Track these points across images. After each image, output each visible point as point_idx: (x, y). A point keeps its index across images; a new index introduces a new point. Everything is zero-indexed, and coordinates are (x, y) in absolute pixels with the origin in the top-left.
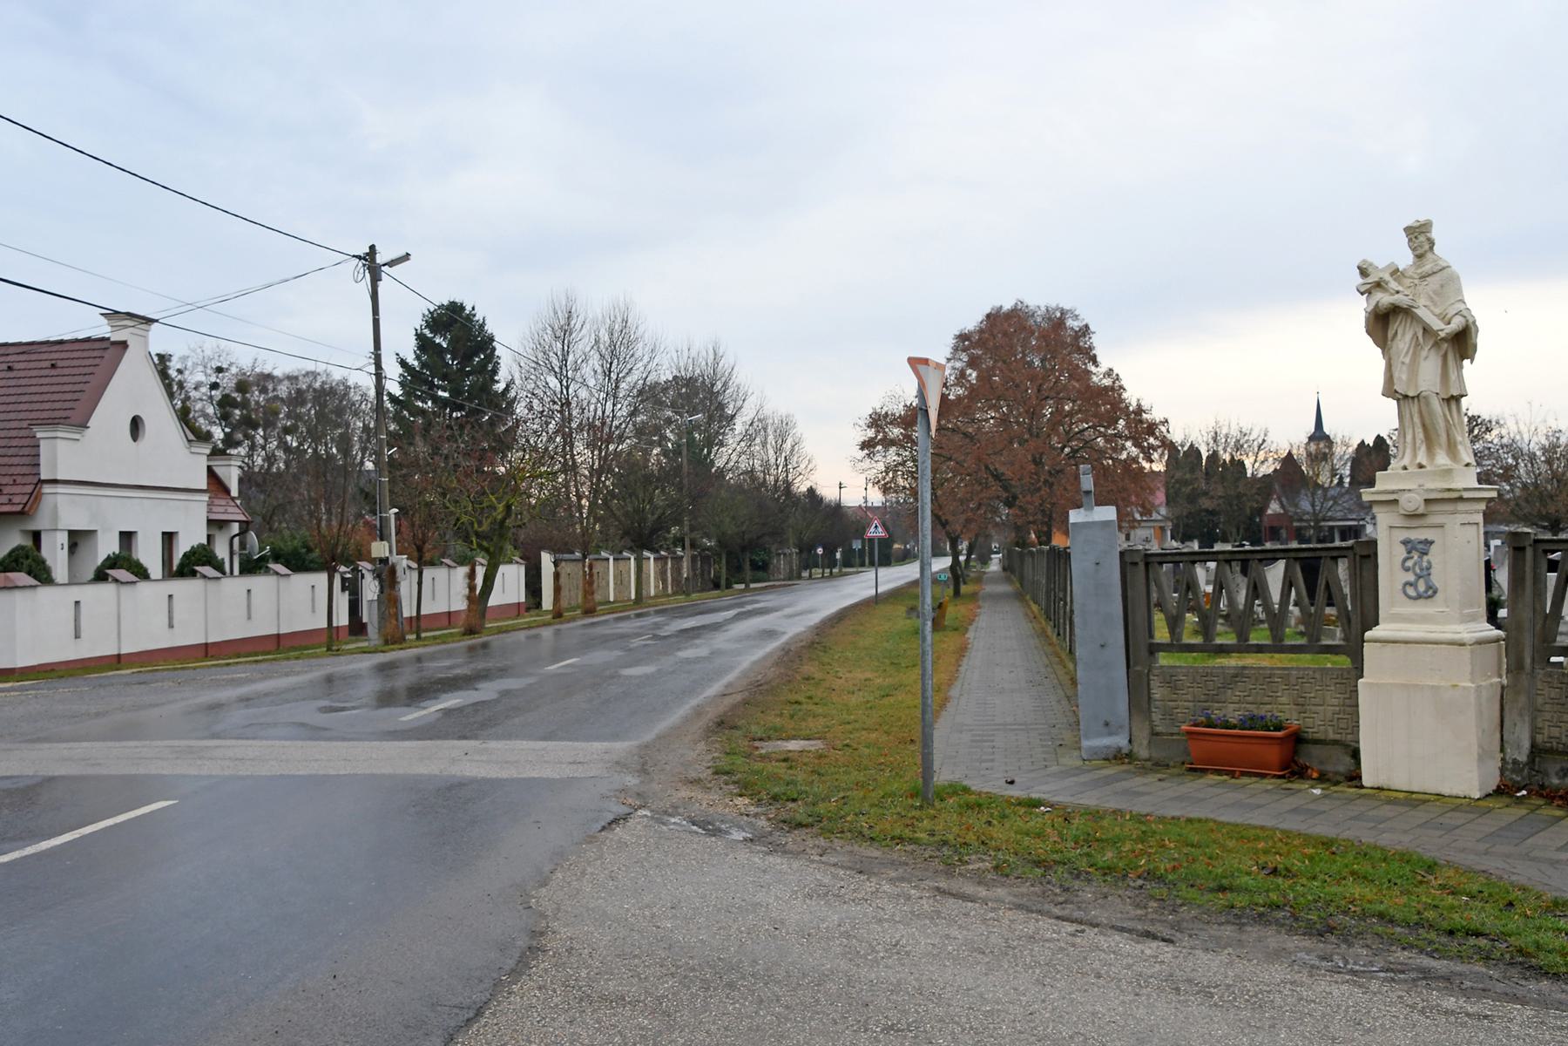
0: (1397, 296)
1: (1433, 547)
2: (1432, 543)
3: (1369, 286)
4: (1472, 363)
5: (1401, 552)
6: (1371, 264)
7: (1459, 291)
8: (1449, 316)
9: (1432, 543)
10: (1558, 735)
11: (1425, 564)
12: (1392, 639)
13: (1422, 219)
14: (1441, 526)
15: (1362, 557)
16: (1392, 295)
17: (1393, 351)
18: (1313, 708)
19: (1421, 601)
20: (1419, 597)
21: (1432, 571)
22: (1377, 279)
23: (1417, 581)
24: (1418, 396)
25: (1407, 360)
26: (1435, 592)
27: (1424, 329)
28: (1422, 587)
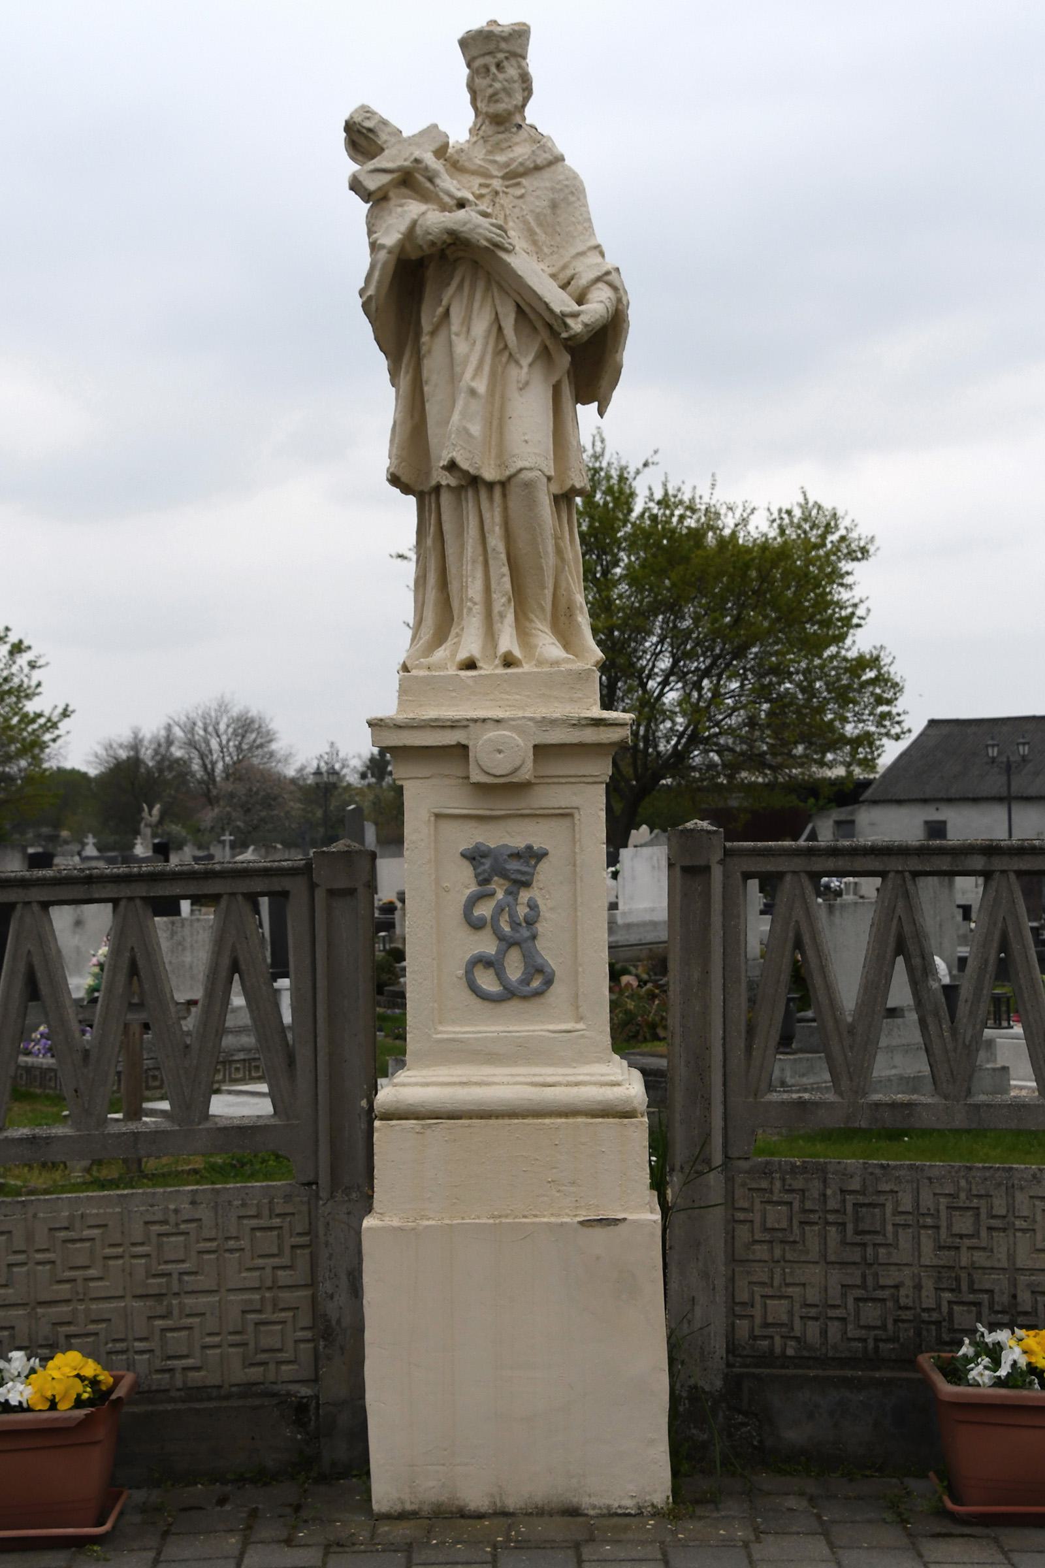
0: (461, 214)
1: (543, 866)
2: (540, 856)
3: (385, 178)
4: (601, 412)
5: (463, 879)
6: (385, 123)
7: (589, 228)
8: (584, 280)
9: (540, 856)
10: (784, 1318)
11: (522, 911)
12: (449, 1107)
13: (507, 19)
14: (566, 815)
15: (332, 893)
16: (444, 208)
17: (433, 366)
18: (189, 1301)
19: (513, 1006)
20: (509, 994)
21: (540, 927)
22: (400, 163)
23: (502, 953)
24: (504, 484)
25: (481, 387)
26: (549, 982)
27: (519, 308)
28: (514, 970)
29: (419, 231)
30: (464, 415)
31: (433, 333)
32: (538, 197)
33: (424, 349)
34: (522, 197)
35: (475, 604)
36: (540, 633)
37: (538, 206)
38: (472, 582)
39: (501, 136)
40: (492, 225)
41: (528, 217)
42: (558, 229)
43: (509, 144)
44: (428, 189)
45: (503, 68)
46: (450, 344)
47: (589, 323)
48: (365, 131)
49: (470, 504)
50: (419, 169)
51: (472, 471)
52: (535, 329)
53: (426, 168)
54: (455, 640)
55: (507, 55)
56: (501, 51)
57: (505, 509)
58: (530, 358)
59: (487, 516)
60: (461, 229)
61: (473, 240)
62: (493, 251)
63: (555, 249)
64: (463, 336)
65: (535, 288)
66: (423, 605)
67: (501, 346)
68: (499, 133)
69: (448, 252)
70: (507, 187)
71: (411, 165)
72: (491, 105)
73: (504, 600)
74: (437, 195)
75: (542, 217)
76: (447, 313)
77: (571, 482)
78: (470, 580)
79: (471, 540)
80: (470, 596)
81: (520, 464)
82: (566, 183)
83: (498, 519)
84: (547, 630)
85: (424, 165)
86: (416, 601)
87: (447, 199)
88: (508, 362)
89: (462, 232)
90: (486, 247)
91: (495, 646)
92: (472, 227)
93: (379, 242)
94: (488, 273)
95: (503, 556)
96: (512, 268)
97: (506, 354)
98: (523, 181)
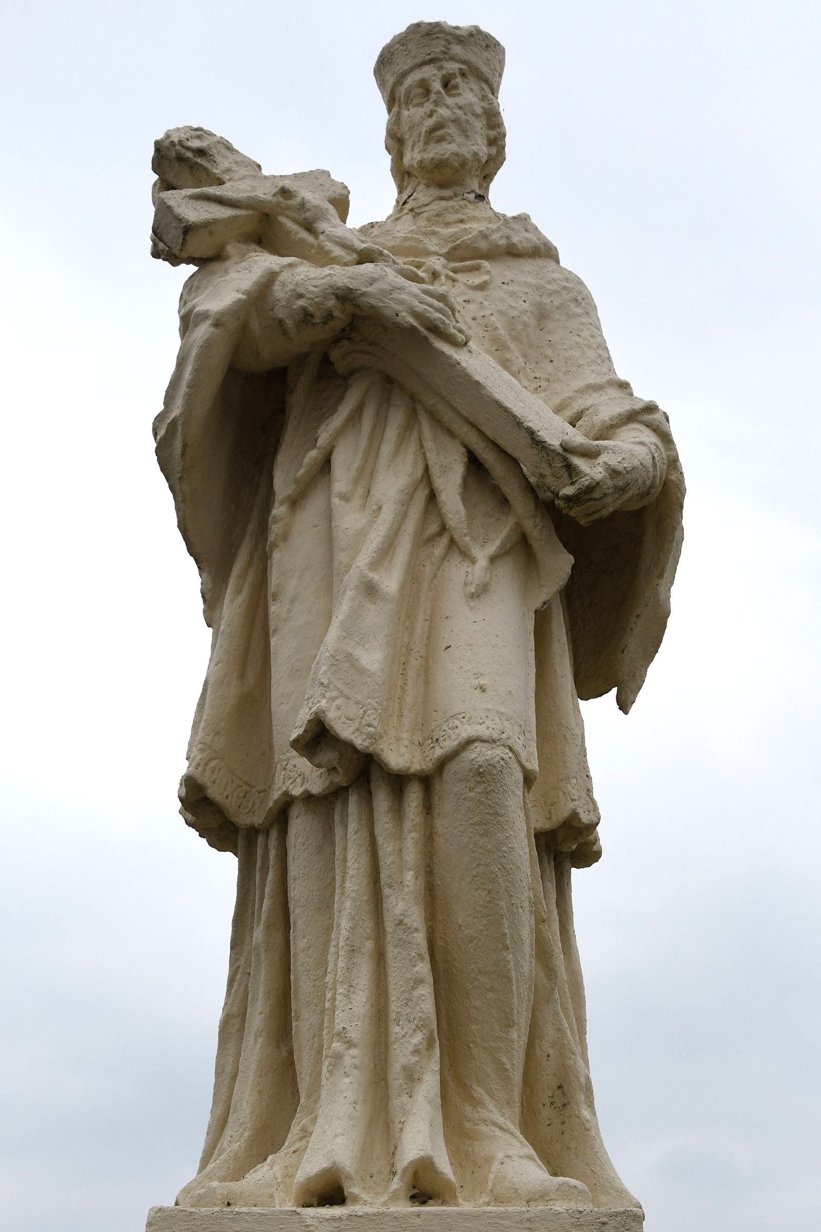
4: (624, 705)
29: (279, 292)
30: (350, 631)
31: (295, 502)
32: (512, 294)
33: (275, 529)
34: (482, 287)
35: (350, 1044)
36: (498, 1132)
38: (347, 996)
39: (444, 204)
40: (426, 292)
42: (549, 352)
43: (459, 216)
44: (303, 240)
45: (456, 87)
46: (329, 516)
47: (620, 468)
48: (189, 154)
49: (352, 826)
50: (288, 208)
51: (360, 742)
52: (504, 502)
53: (303, 206)
54: (297, 1145)
55: (463, 67)
56: (452, 59)
57: (429, 838)
58: (492, 548)
59: (386, 848)
60: (364, 289)
61: (388, 313)
62: (426, 338)
63: (544, 384)
64: (356, 502)
65: (509, 404)
66: (234, 1078)
67: (434, 528)
68: (442, 198)
69: (335, 354)
70: (455, 271)
71: (274, 199)
72: (431, 146)
73: (417, 1039)
74: (321, 248)
75: (519, 327)
76: (325, 466)
77: (571, 805)
78: (340, 990)
79: (348, 904)
80: (338, 1027)
81: (467, 731)
82: (565, 284)
83: (411, 854)
84: (517, 1132)
85: (298, 199)
86: (219, 1072)
87: (337, 251)
88: (444, 558)
90: (413, 328)
91: (393, 1152)
92: (388, 287)
93: (197, 309)
94: (413, 398)
95: (420, 938)
96: (464, 369)
97: (445, 540)
98: (485, 264)
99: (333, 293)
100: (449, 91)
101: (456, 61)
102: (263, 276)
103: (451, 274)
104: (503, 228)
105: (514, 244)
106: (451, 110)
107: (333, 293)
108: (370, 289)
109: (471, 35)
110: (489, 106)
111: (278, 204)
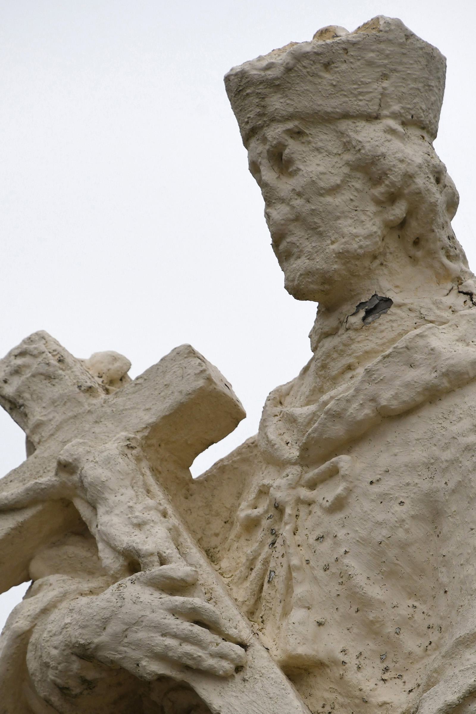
29: (32, 665)
37: (379, 524)
40: (175, 612)
41: (346, 561)
45: (290, 162)
55: (290, 125)
60: (96, 640)
70: (312, 485)
75: (392, 553)
89: (98, 647)
90: (161, 678)
99: (72, 654)
100: (287, 168)
101: (279, 121)
102: (8, 647)
103: (304, 493)
104: (367, 386)
105: (384, 407)
106: (288, 204)
107: (72, 654)
108: (104, 638)
109: (289, 70)
110: (358, 156)
111: (63, 485)
